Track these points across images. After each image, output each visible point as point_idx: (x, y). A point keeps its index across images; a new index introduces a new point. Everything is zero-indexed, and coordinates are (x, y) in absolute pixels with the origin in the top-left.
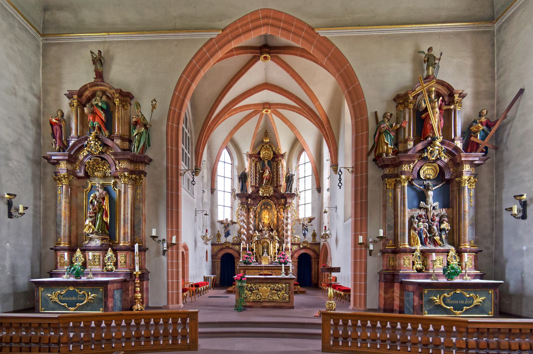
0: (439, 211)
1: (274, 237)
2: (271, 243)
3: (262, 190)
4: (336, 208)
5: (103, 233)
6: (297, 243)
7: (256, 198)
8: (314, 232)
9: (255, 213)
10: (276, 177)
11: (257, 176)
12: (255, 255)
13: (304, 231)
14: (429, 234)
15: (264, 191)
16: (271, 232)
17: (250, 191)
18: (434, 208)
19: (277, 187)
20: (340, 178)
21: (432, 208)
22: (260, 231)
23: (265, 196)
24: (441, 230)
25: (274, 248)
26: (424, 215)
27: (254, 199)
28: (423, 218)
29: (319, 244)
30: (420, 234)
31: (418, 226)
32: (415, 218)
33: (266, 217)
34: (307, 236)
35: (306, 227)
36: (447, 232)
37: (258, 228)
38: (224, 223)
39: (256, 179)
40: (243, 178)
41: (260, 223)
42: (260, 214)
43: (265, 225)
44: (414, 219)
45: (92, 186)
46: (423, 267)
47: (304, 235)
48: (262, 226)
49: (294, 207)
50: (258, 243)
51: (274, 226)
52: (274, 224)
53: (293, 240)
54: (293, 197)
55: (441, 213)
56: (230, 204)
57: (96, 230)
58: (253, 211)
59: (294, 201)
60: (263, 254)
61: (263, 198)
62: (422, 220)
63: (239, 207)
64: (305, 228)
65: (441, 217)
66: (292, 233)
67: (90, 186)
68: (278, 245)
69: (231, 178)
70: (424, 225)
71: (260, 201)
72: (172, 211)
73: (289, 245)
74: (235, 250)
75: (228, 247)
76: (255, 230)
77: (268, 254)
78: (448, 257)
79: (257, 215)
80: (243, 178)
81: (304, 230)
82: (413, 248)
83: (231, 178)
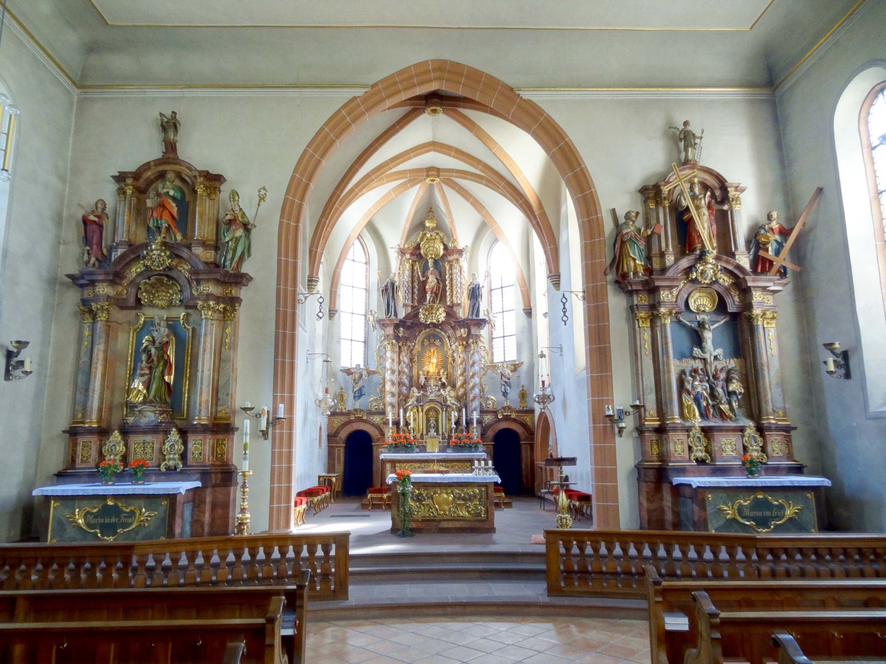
0: (724, 363)
1: (449, 399)
2: (443, 411)
3: (424, 312)
4: (561, 349)
5: (163, 402)
6: (492, 410)
7: (413, 327)
8: (523, 390)
9: (412, 354)
10: (450, 289)
11: (415, 287)
12: (412, 434)
13: (503, 387)
14: (711, 401)
15: (429, 314)
16: (442, 390)
17: (402, 315)
18: (716, 358)
19: (451, 307)
20: (564, 308)
21: (712, 358)
22: (422, 388)
23: (432, 323)
24: (730, 394)
25: (450, 420)
26: (701, 369)
27: (407, 328)
28: (699, 374)
29: (532, 411)
30: (697, 400)
31: (693, 387)
32: (688, 374)
33: (432, 361)
34: (509, 396)
35: (507, 380)
36: (740, 397)
37: (418, 381)
38: (352, 373)
39: (413, 293)
40: (390, 291)
41: (421, 372)
42: (421, 355)
43: (431, 376)
44: (686, 376)
45: (145, 322)
46: (707, 457)
47: (505, 394)
48: (426, 378)
49: (483, 343)
50: (418, 411)
51: (447, 378)
52: (447, 375)
53: (484, 405)
54: (481, 325)
55: (728, 366)
56: (363, 335)
57: (151, 397)
58: (407, 350)
59: (484, 332)
60: (428, 431)
61: (427, 326)
62: (698, 378)
63: (381, 342)
64: (506, 382)
65: (729, 372)
66: (482, 390)
68: (456, 414)
69: (365, 289)
70: (702, 385)
71: (420, 333)
72: (283, 363)
73: (475, 416)
74: (373, 425)
75: (360, 420)
76: (411, 386)
77: (437, 431)
78: (744, 438)
79: (416, 358)
80: (389, 290)
81: (504, 385)
82: (687, 424)
83: (365, 289)
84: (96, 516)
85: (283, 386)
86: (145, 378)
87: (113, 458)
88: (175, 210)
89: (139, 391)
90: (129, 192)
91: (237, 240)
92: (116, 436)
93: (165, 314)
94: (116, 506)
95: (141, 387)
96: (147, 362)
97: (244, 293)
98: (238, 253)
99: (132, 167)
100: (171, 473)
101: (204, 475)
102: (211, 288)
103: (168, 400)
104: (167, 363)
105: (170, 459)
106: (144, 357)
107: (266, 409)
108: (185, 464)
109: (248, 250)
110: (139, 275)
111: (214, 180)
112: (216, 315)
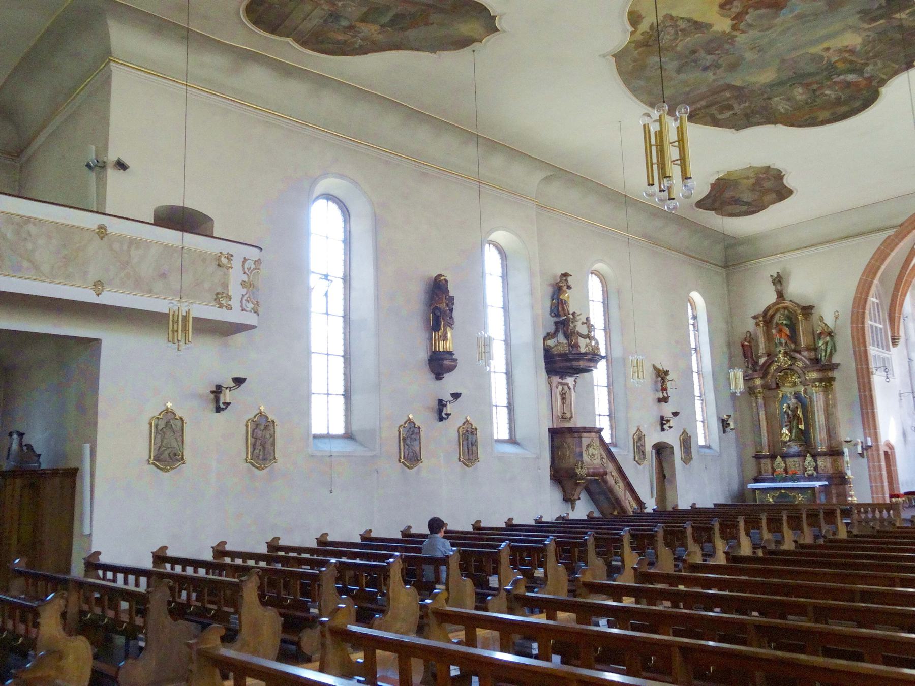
5: (799, 439)
45: (783, 396)
67: (781, 396)
72: (867, 413)
84: (778, 497)
85: (869, 426)
86: (788, 427)
87: (780, 471)
88: (788, 333)
89: (787, 434)
90: (761, 325)
91: (827, 343)
92: (779, 459)
93: (792, 390)
94: (786, 493)
95: (787, 433)
96: (788, 418)
97: (835, 374)
98: (829, 351)
99: (761, 309)
100: (811, 478)
101: (829, 478)
102: (815, 375)
103: (803, 438)
104: (798, 418)
105: (809, 470)
106: (786, 416)
107: (859, 441)
108: (817, 473)
109: (834, 348)
110: (775, 370)
111: (807, 310)
112: (821, 389)
